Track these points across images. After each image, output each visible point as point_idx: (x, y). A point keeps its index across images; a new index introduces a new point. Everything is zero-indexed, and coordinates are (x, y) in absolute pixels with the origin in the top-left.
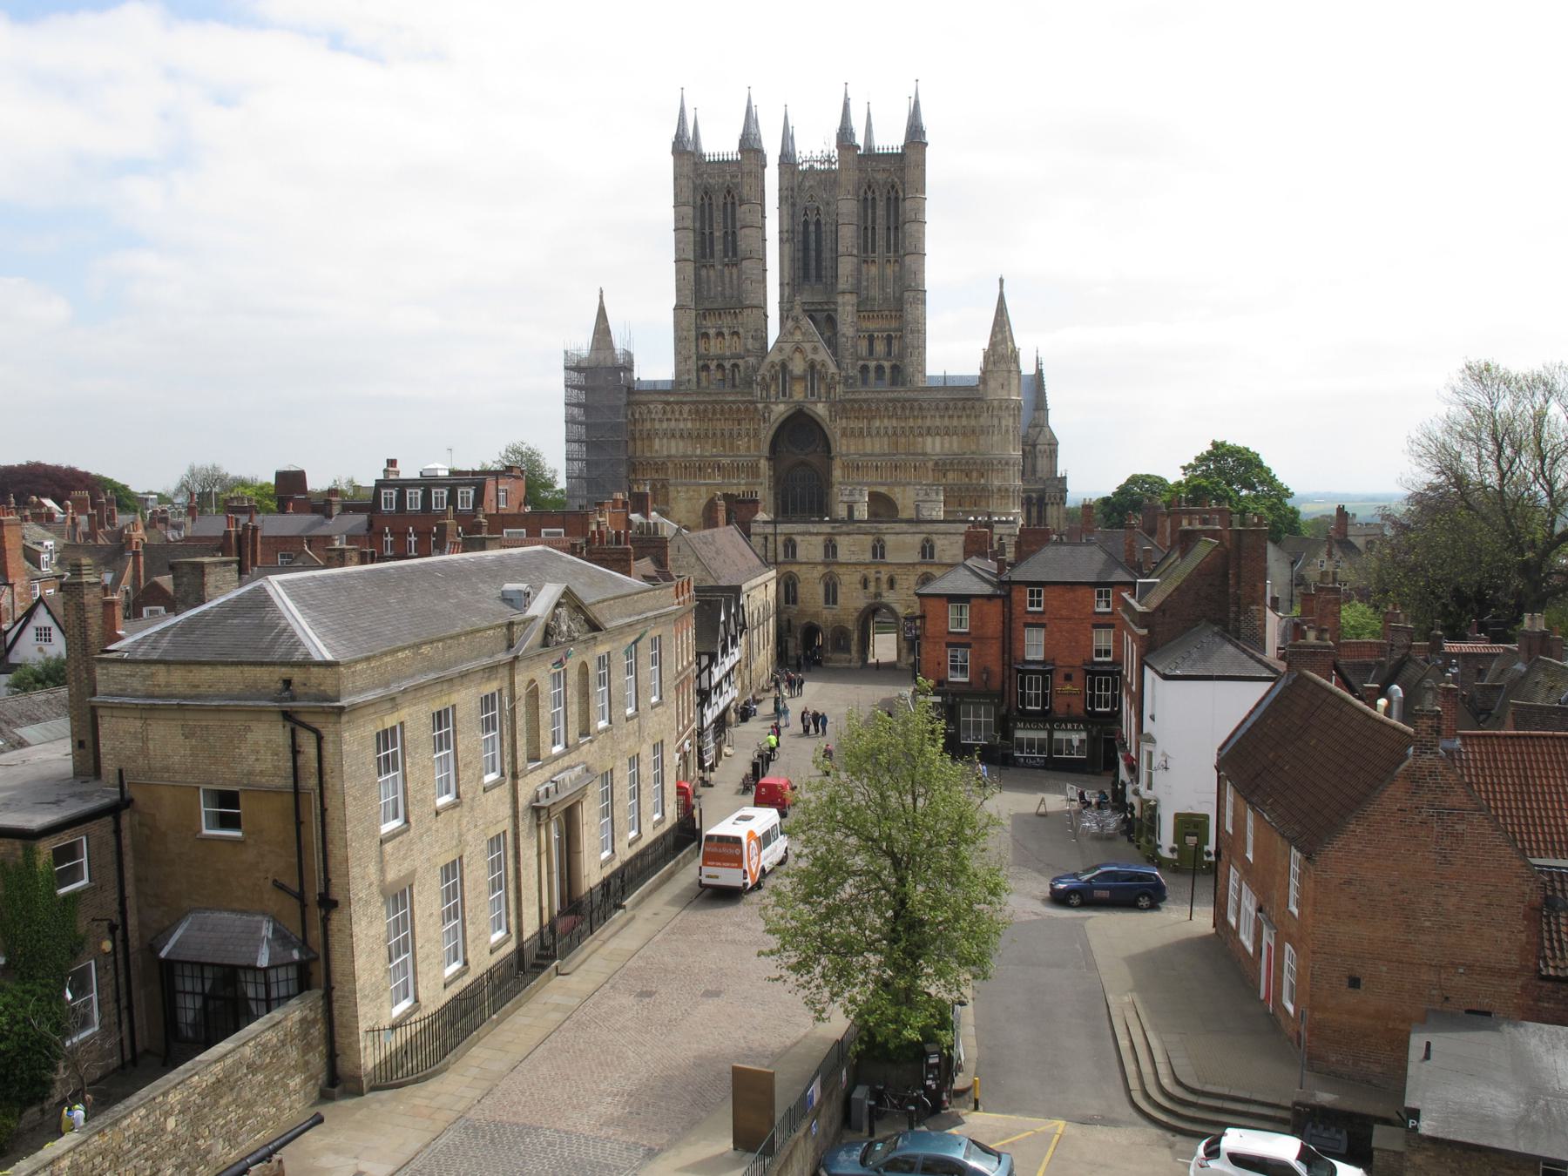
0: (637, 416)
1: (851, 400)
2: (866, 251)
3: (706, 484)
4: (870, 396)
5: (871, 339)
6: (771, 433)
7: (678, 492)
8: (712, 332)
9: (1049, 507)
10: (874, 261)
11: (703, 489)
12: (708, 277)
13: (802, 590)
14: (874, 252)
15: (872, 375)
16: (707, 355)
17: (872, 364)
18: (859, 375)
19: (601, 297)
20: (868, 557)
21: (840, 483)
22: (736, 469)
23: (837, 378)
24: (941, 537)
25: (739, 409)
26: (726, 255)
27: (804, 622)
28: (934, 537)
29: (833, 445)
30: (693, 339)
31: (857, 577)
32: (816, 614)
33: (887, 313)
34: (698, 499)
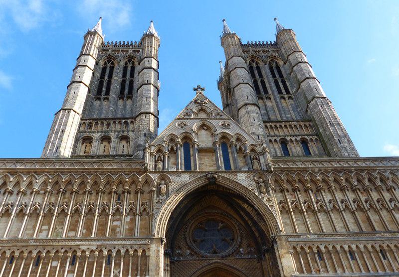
1: (282, 170)
5: (284, 143)
8: (96, 136)
12: (101, 105)
14: (266, 92)
23: (258, 149)
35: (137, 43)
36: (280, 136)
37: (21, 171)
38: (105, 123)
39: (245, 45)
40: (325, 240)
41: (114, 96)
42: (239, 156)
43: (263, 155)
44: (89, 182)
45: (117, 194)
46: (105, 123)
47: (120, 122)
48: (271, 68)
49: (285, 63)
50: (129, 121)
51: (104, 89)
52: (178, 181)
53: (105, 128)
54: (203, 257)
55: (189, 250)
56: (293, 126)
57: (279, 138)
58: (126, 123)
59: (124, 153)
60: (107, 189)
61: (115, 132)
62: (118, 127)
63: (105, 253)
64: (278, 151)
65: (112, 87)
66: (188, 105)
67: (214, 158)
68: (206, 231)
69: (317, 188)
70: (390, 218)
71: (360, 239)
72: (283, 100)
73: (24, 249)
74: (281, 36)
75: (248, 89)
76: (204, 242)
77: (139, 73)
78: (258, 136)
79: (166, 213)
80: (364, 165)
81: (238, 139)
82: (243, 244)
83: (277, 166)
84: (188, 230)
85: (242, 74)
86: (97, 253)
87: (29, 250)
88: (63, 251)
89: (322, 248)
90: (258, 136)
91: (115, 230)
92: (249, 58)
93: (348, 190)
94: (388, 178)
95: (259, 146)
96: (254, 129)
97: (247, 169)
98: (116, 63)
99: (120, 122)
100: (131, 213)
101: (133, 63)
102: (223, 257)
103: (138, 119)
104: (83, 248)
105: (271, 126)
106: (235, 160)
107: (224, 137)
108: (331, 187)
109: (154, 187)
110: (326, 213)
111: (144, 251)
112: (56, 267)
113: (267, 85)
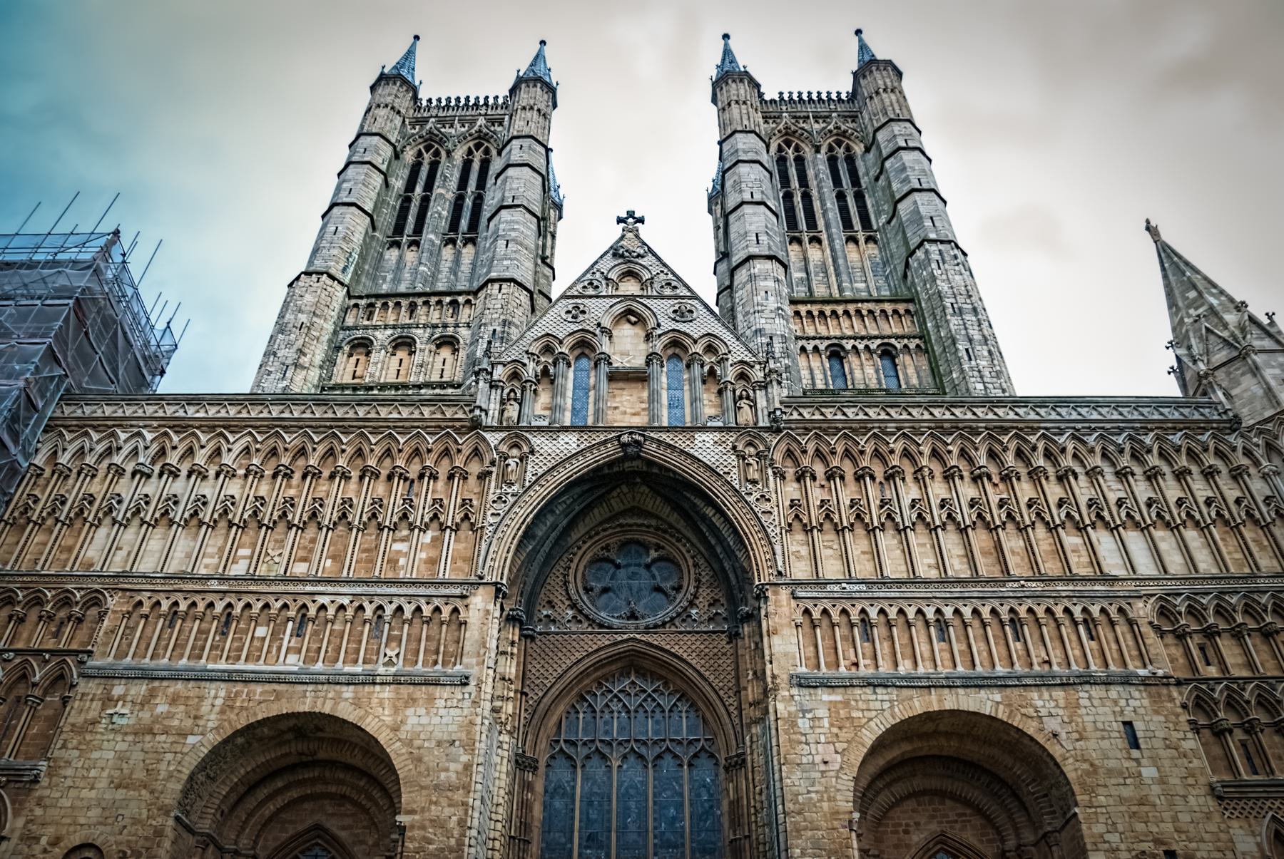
1: (806, 426)
3: (228, 678)
5: (837, 354)
6: (524, 512)
8: (382, 337)
10: (816, 240)
11: (217, 693)
14: (812, 224)
23: (757, 374)
29: (759, 552)
30: (325, 338)
33: (871, 306)
34: (185, 736)
35: (500, 101)
36: (828, 338)
37: (197, 424)
39: (773, 101)
40: (882, 595)
41: (432, 236)
42: (708, 390)
43: (766, 388)
44: (343, 451)
45: (406, 479)
48: (832, 161)
49: (867, 150)
50: (461, 299)
51: (411, 220)
52: (550, 451)
54: (601, 626)
55: (572, 609)
56: (865, 312)
57: (827, 343)
58: (454, 304)
59: (443, 380)
60: (384, 468)
61: (425, 326)
62: (435, 316)
63: (369, 613)
64: (819, 376)
65: (429, 213)
66: (596, 262)
67: (645, 394)
68: (618, 567)
69: (886, 472)
70: (1050, 544)
71: (967, 595)
72: (851, 246)
73: (197, 598)
74: (864, 77)
75: (762, 218)
76: (611, 594)
77: (496, 178)
78: (771, 338)
79: (513, 525)
80: (1012, 416)
81: (710, 349)
82: (701, 599)
83: (795, 416)
84: (573, 566)
85: (753, 180)
86: (350, 612)
87: (207, 602)
88: (279, 604)
89: (873, 613)
90: (771, 338)
91: (397, 561)
92: (778, 135)
93: (962, 477)
94: (1063, 450)
95: (757, 367)
96: (763, 321)
97: (720, 424)
98: (443, 153)
99: (439, 303)
100: (435, 525)
101: (487, 151)
102: (647, 627)
103: (482, 294)
104: (322, 600)
105: (809, 313)
106: (694, 400)
107: (677, 344)
108: (921, 469)
109: (493, 463)
110: (899, 531)
111: (456, 610)
112: (264, 639)
113: (817, 205)
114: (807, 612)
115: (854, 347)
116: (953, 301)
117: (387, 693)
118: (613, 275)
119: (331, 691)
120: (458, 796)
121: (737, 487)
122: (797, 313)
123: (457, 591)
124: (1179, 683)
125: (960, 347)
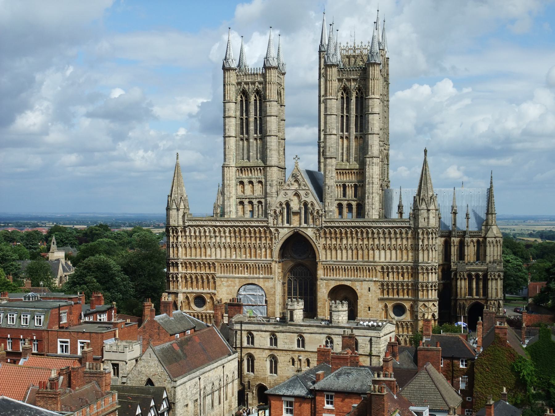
0: (197, 234)
1: (327, 227)
2: (342, 131)
4: (341, 224)
5: (344, 187)
6: (279, 246)
7: (222, 281)
8: (246, 181)
9: (490, 283)
11: (237, 280)
13: (255, 364)
14: (347, 131)
15: (345, 210)
16: (242, 196)
17: (345, 203)
18: (337, 211)
19: (177, 158)
20: (295, 347)
21: (322, 279)
22: (257, 268)
23: (320, 212)
24: (336, 336)
25: (260, 231)
26: (256, 133)
27: (258, 383)
28: (332, 336)
29: (317, 255)
31: (288, 358)
32: (264, 379)
34: (234, 287)
38: (249, 169)
46: (249, 169)
47: (257, 169)
50: (261, 168)
53: (250, 175)
57: (342, 183)
63: (257, 266)
64: (339, 193)
89: (334, 267)
111: (270, 266)
114: (324, 266)
115: (348, 185)
116: (368, 179)
117: (262, 280)
118: (293, 182)
119: (254, 280)
120: (274, 296)
121: (314, 241)
122: (337, 172)
123: (270, 262)
124: (379, 282)
125: (366, 195)
